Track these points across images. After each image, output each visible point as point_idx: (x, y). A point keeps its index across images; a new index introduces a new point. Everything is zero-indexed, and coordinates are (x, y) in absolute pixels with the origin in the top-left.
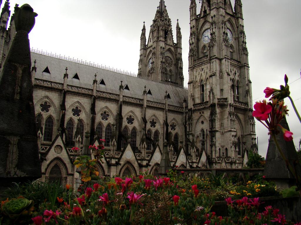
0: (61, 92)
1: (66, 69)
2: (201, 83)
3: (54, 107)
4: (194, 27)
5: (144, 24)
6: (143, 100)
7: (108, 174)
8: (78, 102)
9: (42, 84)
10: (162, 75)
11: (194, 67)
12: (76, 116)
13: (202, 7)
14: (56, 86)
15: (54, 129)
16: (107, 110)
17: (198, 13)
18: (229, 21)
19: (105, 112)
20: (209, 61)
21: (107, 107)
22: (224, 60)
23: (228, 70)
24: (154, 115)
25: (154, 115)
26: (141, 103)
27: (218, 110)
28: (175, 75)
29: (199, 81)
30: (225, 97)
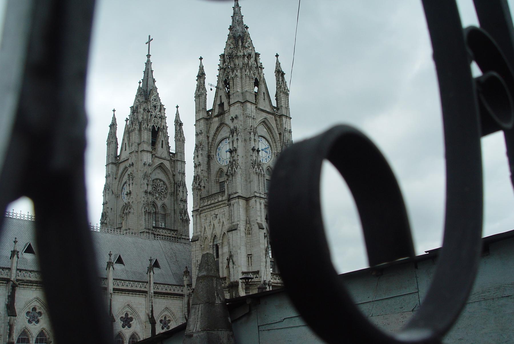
2: (213, 242)
4: (201, 133)
5: (114, 115)
6: (107, 279)
10: (147, 217)
11: (201, 211)
13: (216, 96)
17: (209, 106)
18: (264, 122)
19: (34, 309)
20: (226, 202)
22: (253, 200)
23: (261, 219)
24: (128, 305)
25: (128, 305)
28: (172, 214)
29: (209, 237)
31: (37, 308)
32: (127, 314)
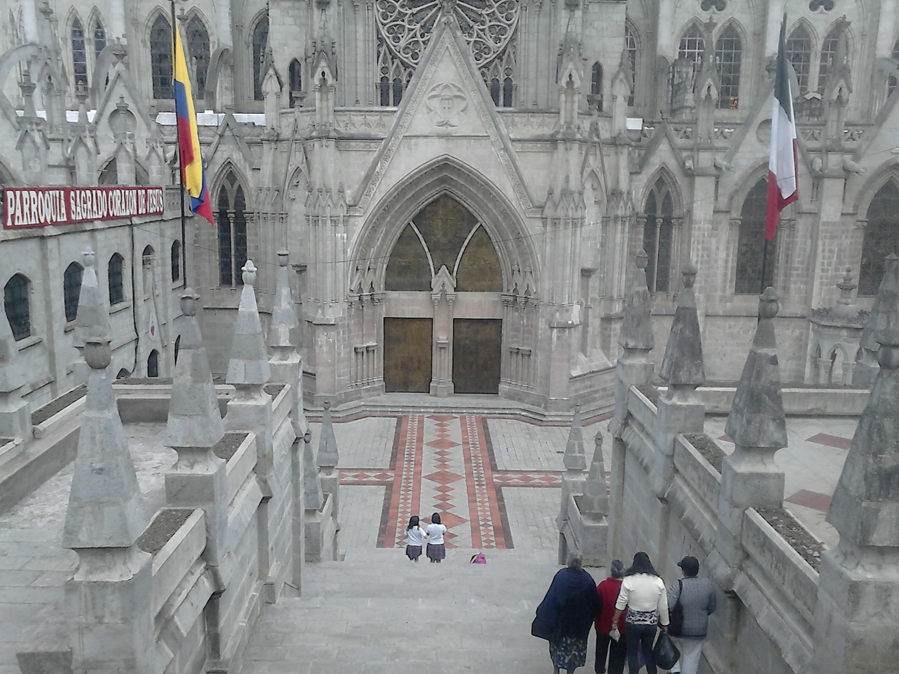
15: (743, 67)
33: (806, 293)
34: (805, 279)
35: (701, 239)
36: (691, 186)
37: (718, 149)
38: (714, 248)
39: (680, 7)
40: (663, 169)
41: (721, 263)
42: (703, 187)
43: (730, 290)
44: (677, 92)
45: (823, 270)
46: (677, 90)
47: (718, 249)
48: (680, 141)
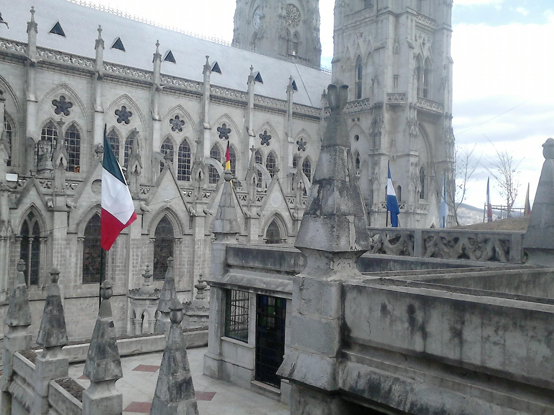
0: (91, 76)
1: (100, 30)
3: (80, 106)
7: (190, 232)
8: (126, 96)
9: (53, 59)
12: (124, 125)
14: (83, 65)
15: (81, 149)
16: (181, 112)
19: (177, 117)
20: (374, 18)
21: (180, 106)
23: (411, 37)
25: (268, 122)
26: (244, 99)
27: (387, 116)
29: (352, 56)
30: (401, 90)
31: (180, 116)
32: (265, 132)
33: (125, 280)
34: (124, 272)
35: (59, 250)
36: (52, 217)
37: (69, 196)
38: (68, 255)
39: (41, 110)
40: (33, 207)
41: (73, 264)
42: (60, 218)
43: (80, 281)
44: (41, 159)
45: (133, 267)
46: (40, 158)
47: (70, 256)
48: (44, 190)
